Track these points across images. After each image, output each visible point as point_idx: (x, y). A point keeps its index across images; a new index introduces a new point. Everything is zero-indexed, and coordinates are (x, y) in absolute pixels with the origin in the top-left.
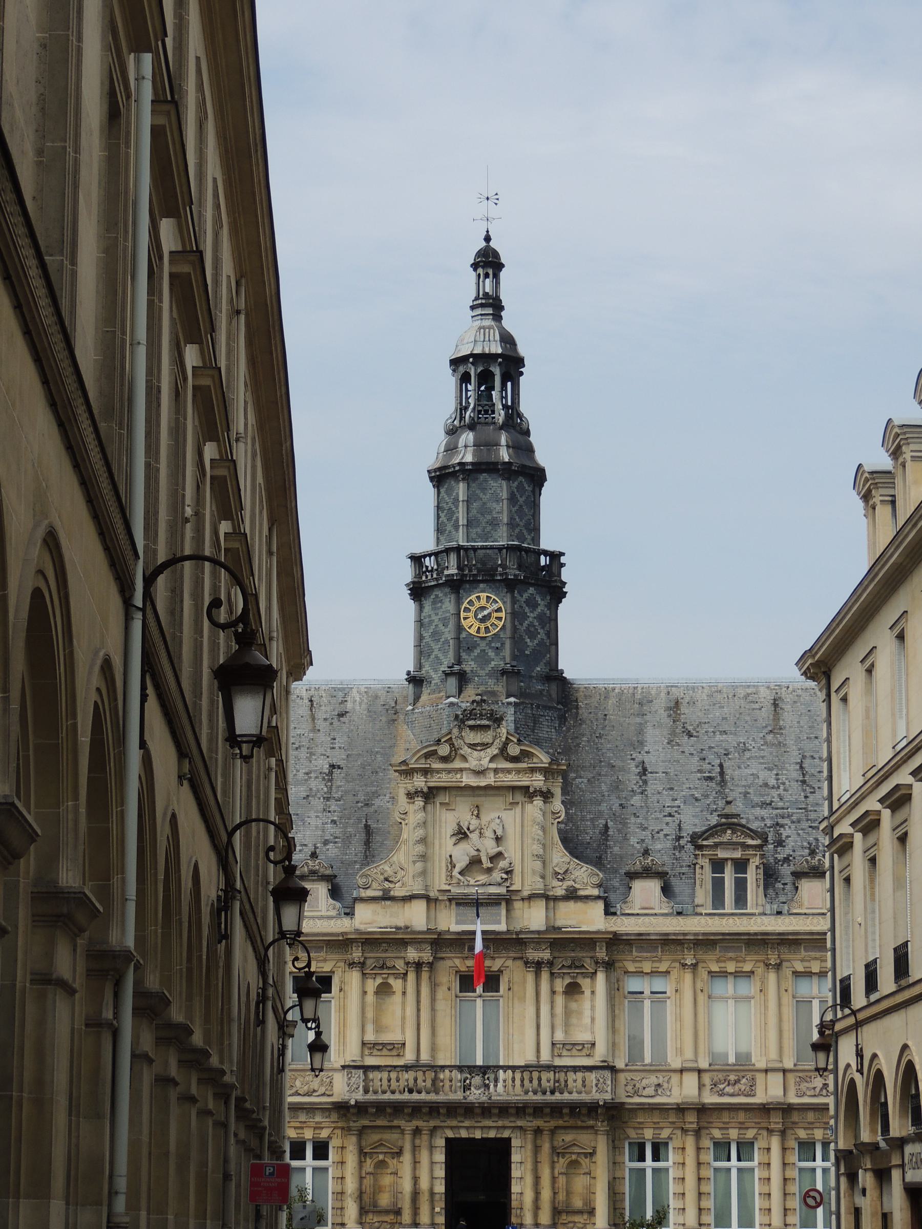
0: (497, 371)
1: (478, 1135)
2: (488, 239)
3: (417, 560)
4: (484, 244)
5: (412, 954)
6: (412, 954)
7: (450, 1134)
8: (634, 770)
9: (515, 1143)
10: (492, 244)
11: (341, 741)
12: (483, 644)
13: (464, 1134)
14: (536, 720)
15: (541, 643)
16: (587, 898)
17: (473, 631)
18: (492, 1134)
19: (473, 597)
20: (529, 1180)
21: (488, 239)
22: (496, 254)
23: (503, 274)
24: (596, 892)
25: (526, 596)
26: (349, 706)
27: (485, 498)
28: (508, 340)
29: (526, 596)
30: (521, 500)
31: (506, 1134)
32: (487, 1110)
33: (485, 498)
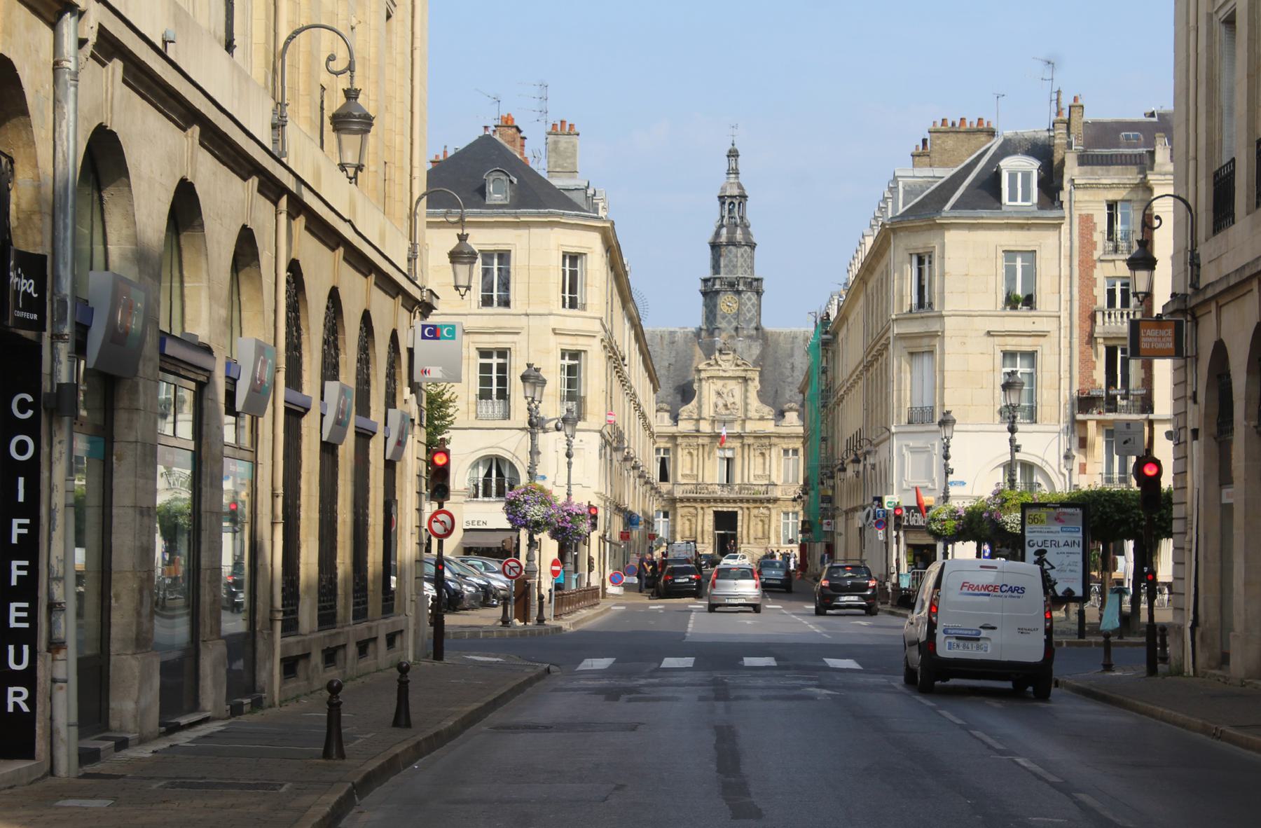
0: (736, 202)
1: (725, 510)
2: (733, 145)
3: (705, 281)
4: (730, 147)
5: (700, 441)
6: (700, 441)
7: (715, 509)
8: (788, 366)
9: (740, 512)
10: (736, 146)
11: (674, 354)
12: (729, 317)
13: (720, 509)
14: (750, 346)
15: (753, 314)
16: (767, 419)
17: (725, 311)
18: (730, 510)
19: (726, 297)
20: (745, 527)
21: (733, 145)
22: (737, 151)
23: (739, 159)
24: (771, 417)
25: (747, 296)
26: (676, 339)
27: (731, 256)
28: (740, 187)
29: (747, 296)
30: (745, 256)
31: (736, 510)
32: (728, 501)
33: (731, 256)
